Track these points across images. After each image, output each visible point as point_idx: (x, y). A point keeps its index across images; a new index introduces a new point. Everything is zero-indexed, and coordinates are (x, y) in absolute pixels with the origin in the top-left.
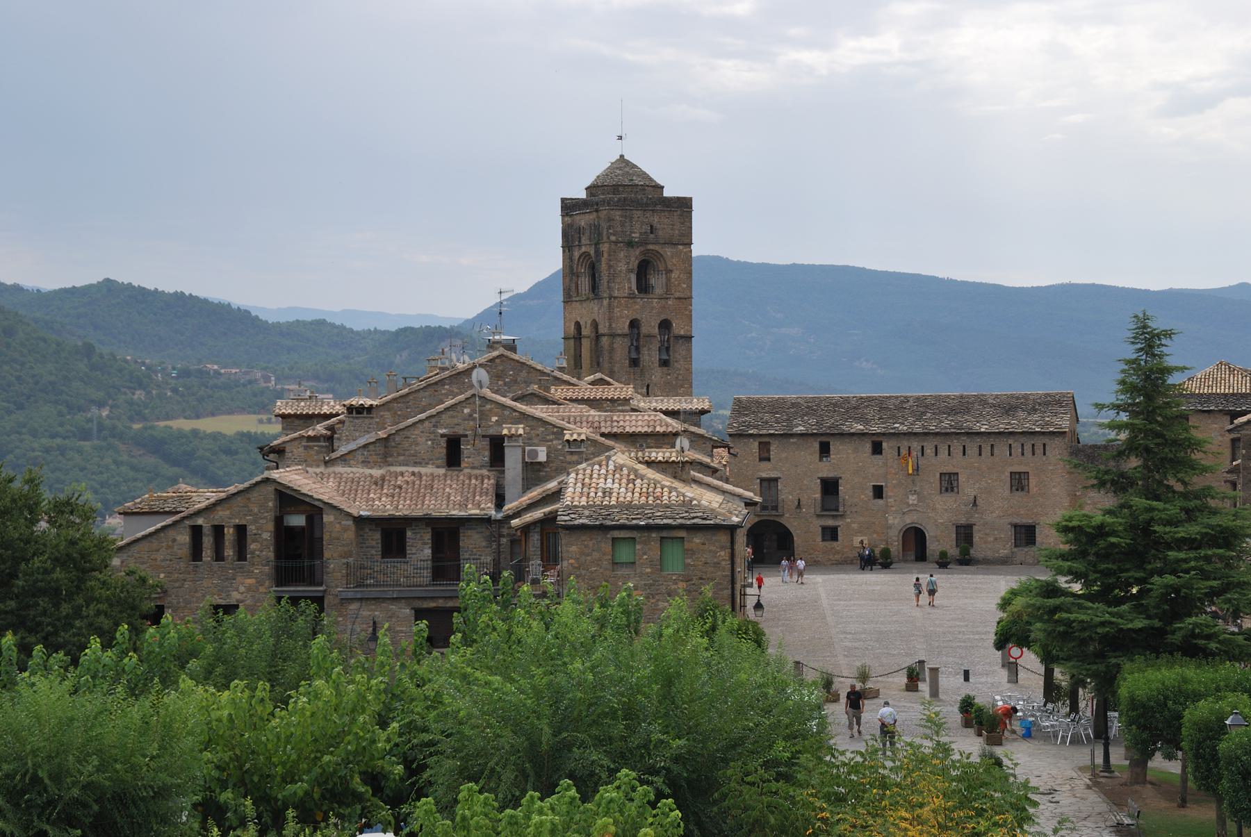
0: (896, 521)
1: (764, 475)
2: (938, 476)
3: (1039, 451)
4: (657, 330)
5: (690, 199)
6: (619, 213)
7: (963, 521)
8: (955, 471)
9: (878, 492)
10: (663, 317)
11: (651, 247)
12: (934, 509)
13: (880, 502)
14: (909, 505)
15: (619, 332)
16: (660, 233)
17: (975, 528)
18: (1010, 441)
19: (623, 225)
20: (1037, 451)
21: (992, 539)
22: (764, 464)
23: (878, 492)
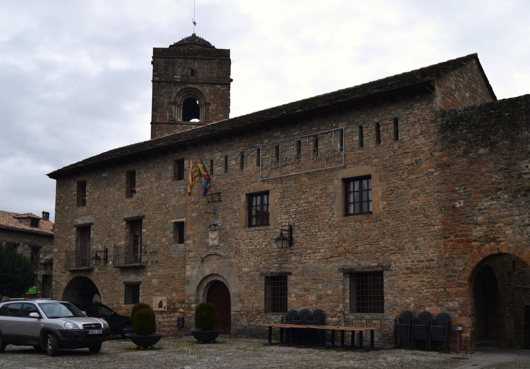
0: (194, 273)
1: (80, 222)
2: (243, 198)
3: (387, 134)
5: (228, 51)
6: (164, 60)
7: (274, 269)
8: (266, 187)
12: (237, 252)
13: (181, 246)
14: (209, 247)
16: (200, 75)
17: (291, 279)
20: (384, 135)
21: (314, 298)
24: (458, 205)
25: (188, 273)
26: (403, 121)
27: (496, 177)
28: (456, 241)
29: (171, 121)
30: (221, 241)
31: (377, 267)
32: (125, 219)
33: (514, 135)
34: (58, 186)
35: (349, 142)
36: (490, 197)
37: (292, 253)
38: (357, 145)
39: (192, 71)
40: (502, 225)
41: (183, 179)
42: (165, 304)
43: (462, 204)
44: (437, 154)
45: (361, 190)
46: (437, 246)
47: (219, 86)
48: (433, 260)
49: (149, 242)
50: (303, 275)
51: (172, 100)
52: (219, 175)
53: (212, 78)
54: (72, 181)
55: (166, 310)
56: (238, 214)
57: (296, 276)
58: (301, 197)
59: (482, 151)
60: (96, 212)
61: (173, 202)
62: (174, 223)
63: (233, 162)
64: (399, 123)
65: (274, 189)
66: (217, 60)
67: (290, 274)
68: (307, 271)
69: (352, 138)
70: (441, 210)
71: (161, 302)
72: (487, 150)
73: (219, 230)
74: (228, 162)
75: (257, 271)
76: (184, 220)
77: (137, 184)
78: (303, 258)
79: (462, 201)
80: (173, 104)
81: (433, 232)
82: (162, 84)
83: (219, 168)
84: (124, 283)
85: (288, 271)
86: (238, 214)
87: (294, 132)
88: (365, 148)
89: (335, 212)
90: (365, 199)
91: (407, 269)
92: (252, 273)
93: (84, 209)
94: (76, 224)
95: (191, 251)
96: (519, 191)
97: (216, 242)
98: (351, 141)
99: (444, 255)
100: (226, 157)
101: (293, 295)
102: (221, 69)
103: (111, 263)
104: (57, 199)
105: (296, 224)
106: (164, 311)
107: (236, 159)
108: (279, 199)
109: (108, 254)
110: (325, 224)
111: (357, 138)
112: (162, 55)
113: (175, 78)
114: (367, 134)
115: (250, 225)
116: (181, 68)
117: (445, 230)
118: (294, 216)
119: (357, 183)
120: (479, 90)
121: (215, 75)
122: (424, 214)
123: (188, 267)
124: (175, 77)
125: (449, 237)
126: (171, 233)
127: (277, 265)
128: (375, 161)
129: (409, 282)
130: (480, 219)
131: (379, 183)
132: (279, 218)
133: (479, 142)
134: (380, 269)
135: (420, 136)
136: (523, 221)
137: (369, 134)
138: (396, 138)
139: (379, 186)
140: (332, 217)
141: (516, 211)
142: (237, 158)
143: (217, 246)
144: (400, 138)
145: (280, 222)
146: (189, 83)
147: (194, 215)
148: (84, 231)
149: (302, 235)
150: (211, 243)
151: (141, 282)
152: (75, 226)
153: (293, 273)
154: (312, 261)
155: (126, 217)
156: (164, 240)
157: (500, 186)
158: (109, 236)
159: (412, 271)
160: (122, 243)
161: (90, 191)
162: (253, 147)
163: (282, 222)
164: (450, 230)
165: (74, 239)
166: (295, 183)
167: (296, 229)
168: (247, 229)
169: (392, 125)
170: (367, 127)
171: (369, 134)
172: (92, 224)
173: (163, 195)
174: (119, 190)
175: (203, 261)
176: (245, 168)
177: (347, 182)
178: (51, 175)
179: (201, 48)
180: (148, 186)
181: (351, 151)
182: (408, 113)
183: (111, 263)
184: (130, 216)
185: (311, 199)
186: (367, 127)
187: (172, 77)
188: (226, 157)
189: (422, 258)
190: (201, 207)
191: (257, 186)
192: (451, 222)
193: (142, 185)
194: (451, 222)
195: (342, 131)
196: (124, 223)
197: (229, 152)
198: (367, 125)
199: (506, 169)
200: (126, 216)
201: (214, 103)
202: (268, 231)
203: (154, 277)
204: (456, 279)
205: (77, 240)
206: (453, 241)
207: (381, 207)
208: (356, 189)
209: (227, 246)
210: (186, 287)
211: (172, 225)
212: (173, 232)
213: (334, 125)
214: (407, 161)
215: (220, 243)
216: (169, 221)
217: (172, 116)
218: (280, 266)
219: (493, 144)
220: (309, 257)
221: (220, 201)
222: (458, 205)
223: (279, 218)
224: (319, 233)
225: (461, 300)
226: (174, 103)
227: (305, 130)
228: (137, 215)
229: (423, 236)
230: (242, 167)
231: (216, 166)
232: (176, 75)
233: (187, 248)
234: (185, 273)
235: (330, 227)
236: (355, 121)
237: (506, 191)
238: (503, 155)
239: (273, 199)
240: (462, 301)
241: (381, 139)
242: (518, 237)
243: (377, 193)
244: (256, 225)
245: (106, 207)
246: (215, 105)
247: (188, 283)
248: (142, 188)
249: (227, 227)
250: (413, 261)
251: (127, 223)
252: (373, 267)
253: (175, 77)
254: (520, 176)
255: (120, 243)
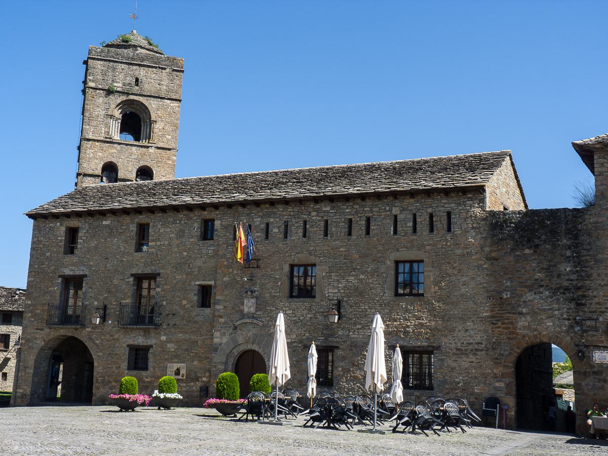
0: (225, 340)
1: (67, 272)
2: (287, 268)
3: (441, 224)
4: (134, 175)
8: (312, 259)
9: (205, 296)
10: (142, 163)
11: (132, 97)
13: (207, 311)
14: (243, 316)
15: (90, 172)
16: (146, 86)
18: (395, 211)
19: (104, 74)
20: (437, 225)
22: (69, 259)
23: (205, 296)
24: (505, 297)
25: (216, 340)
26: (456, 215)
27: (539, 275)
28: (503, 328)
29: (106, 138)
30: (257, 309)
31: (428, 346)
32: (132, 275)
33: (555, 241)
34: (36, 228)
35: (402, 227)
36: (533, 292)
37: (339, 327)
38: (410, 230)
39: (137, 80)
40: (544, 317)
41: (212, 239)
42: (183, 371)
43: (509, 296)
44: (487, 249)
45: (411, 271)
46: (486, 331)
47: (169, 102)
48: (482, 344)
49: (164, 303)
50: (351, 350)
51: (110, 113)
52: (258, 242)
53: (160, 90)
54: (58, 224)
55: (185, 378)
56: (279, 283)
57: (343, 350)
58: (351, 274)
59: (527, 251)
60: (91, 263)
61: (199, 262)
62: (199, 285)
63: (276, 230)
64: (452, 217)
65: (322, 262)
66: (168, 70)
67: (338, 348)
68: (355, 346)
69: (406, 224)
70: (490, 299)
71: (178, 370)
72: (532, 251)
73: (256, 297)
74: (270, 229)
75: (300, 343)
76: (212, 283)
77: (150, 238)
78: (351, 333)
79: (508, 293)
80: (111, 118)
81: (483, 318)
82: (98, 91)
83: (259, 234)
84: (128, 346)
85: (334, 344)
86: (279, 283)
87: (346, 209)
88: (418, 235)
89: (386, 291)
90: (415, 280)
91: (458, 349)
92: (294, 344)
93: (74, 259)
94: (61, 274)
95: (221, 317)
96: (559, 289)
97: (252, 310)
98: (404, 226)
99: (492, 340)
100: (268, 225)
101: (340, 369)
102: (171, 80)
103: (110, 322)
104: (33, 243)
105: (345, 299)
106: (181, 380)
107: (279, 227)
108: (326, 273)
109: (107, 312)
110: (375, 301)
111: (411, 224)
112: (101, 56)
113: (115, 86)
114: (421, 222)
115: (291, 296)
116: (123, 74)
117: (492, 317)
118: (343, 291)
119: (407, 266)
120: (511, 184)
121: (165, 87)
122: (473, 301)
123: (217, 334)
124: (115, 84)
125: (496, 323)
126: (195, 295)
127: (323, 338)
128: (427, 247)
129: (458, 362)
130: (524, 310)
131: (430, 269)
132: (326, 292)
133: (524, 243)
134: (431, 349)
135: (472, 231)
136: (562, 315)
137: (423, 222)
138: (449, 230)
139: (431, 271)
140: (383, 296)
141: (556, 306)
142: (280, 227)
143: (254, 314)
144: (452, 230)
145: (327, 295)
146: (132, 94)
147: (225, 279)
148: (73, 282)
149: (351, 310)
150: (246, 310)
151: (151, 346)
152: (60, 276)
153: (340, 347)
154: (361, 336)
155: (134, 273)
156: (184, 302)
157: (542, 283)
158: (109, 292)
159: (460, 352)
160: (128, 301)
161: (84, 238)
162: (299, 218)
163: (329, 296)
164: (497, 317)
165: (58, 292)
166: (345, 259)
167: (344, 304)
168: (290, 300)
169: (446, 218)
170: (421, 216)
171: (423, 222)
172: (85, 276)
173: (185, 254)
174: (126, 242)
175: (235, 328)
176: (289, 238)
177: (397, 263)
178: (30, 216)
179: (148, 52)
180: (166, 243)
181: (404, 236)
182: (461, 208)
183: (110, 322)
184: (140, 272)
185: (362, 277)
186: (421, 216)
187: (111, 84)
188: (268, 225)
189: (471, 341)
190: (235, 272)
191: (303, 258)
192: (498, 310)
193: (159, 240)
194: (498, 310)
195: (396, 217)
196: (131, 279)
197: (271, 220)
198: (421, 214)
199: (547, 269)
200: (134, 271)
201: (162, 121)
202: (314, 304)
203: (169, 341)
204: (503, 361)
205: (61, 293)
206: (499, 327)
207: (433, 290)
208: (407, 270)
209: (266, 315)
210: (213, 355)
211: (197, 288)
212: (197, 295)
213: (388, 208)
214: (458, 252)
215: (256, 311)
216: (193, 283)
217: (109, 132)
218: (327, 339)
219: (537, 246)
220: (358, 332)
221: (258, 267)
222: (505, 297)
223: (326, 292)
224: (369, 310)
225: (507, 380)
226: (112, 116)
227: (356, 209)
228: (150, 272)
229: (473, 321)
230: (286, 237)
231: (255, 231)
232: (117, 82)
233: (217, 314)
234: (212, 338)
235: (381, 305)
236: (409, 208)
237: (547, 288)
238: (545, 256)
239: (319, 272)
240: (507, 382)
241: (435, 228)
242: (558, 329)
243: (429, 278)
244: (298, 297)
245: (107, 258)
246: (163, 124)
247: (216, 350)
248: (158, 243)
249: (267, 295)
250: (463, 343)
251: (134, 280)
252: (423, 347)
253: (115, 84)
254: (559, 276)
255: (124, 301)
